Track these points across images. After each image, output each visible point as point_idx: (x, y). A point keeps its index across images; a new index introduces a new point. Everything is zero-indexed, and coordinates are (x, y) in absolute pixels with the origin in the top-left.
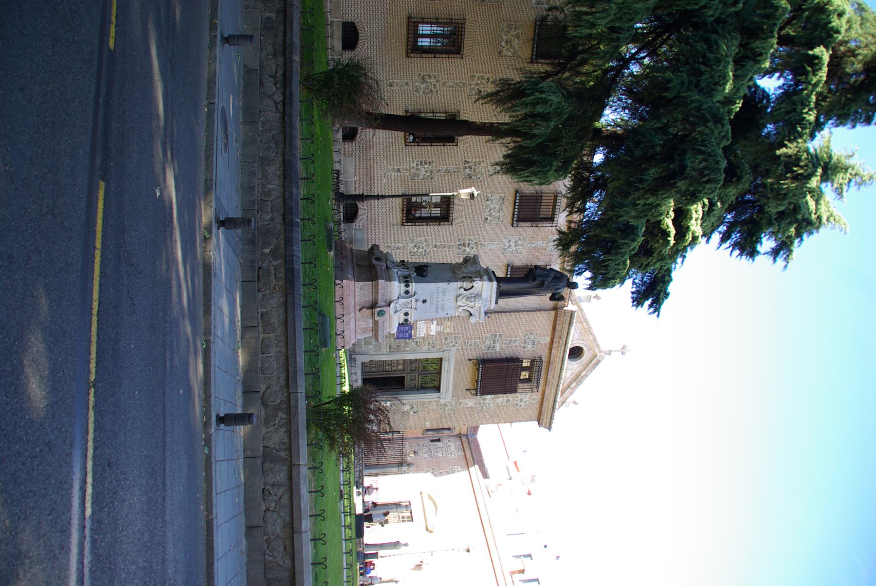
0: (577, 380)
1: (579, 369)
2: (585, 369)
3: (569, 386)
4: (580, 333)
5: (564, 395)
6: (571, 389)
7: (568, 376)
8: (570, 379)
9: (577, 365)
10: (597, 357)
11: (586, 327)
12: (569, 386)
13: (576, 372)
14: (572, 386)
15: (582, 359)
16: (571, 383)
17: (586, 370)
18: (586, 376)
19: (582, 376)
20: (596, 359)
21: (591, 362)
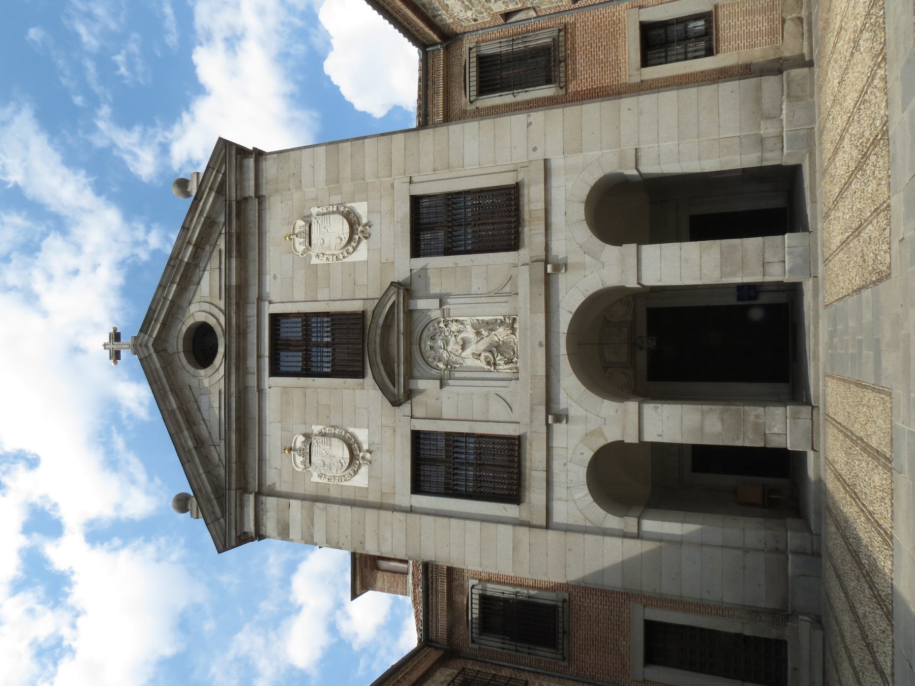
0: (182, 269)
1: (189, 294)
2: (172, 301)
3: (199, 247)
4: (199, 409)
5: (203, 219)
6: (189, 243)
7: (207, 274)
8: (202, 265)
9: (193, 308)
10: (152, 340)
11: (186, 433)
12: (199, 247)
13: (192, 287)
14: (190, 248)
15: (184, 329)
16: (195, 256)
17: (168, 303)
18: (162, 286)
19: (173, 282)
20: (154, 335)
21: (164, 324)
